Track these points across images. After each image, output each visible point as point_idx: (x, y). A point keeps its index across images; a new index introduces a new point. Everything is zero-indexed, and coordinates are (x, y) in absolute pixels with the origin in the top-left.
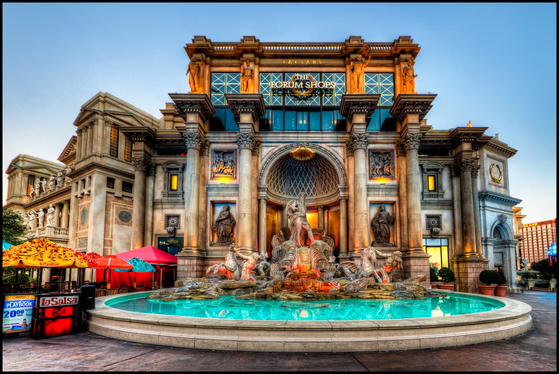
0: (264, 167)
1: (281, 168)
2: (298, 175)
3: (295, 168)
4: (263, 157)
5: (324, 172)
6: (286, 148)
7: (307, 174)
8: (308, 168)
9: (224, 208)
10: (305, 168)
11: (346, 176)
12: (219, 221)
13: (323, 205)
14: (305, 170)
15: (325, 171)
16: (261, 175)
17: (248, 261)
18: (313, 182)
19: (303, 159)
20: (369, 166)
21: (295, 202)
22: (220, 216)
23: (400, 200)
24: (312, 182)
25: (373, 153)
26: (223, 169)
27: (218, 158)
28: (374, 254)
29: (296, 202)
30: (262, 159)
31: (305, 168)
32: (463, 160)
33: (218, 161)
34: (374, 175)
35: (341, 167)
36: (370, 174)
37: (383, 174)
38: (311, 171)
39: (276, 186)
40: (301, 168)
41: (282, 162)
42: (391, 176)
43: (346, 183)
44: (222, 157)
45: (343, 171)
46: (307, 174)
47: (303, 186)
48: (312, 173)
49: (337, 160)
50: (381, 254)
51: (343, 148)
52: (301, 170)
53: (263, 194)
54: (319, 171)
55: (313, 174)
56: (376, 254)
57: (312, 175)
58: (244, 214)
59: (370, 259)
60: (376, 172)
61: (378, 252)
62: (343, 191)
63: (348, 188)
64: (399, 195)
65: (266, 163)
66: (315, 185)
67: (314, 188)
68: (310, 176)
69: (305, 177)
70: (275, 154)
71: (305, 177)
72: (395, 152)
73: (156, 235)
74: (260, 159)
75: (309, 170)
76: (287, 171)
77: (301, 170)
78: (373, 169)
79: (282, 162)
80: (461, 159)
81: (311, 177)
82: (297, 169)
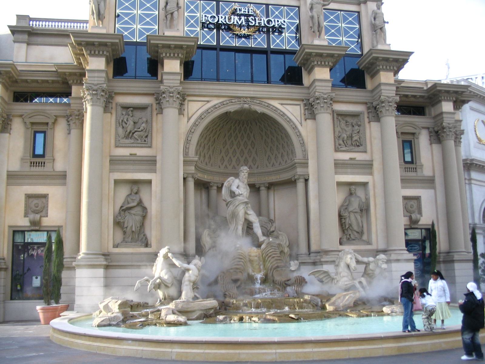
6: (222, 103)
25: (337, 115)
26: (133, 131)
27: (126, 116)
30: (189, 119)
32: (444, 124)
34: (340, 145)
36: (335, 145)
37: (352, 144)
44: (131, 115)
49: (292, 124)
51: (299, 107)
56: (356, 258)
65: (195, 124)
70: (207, 112)
72: (366, 115)
80: (442, 123)
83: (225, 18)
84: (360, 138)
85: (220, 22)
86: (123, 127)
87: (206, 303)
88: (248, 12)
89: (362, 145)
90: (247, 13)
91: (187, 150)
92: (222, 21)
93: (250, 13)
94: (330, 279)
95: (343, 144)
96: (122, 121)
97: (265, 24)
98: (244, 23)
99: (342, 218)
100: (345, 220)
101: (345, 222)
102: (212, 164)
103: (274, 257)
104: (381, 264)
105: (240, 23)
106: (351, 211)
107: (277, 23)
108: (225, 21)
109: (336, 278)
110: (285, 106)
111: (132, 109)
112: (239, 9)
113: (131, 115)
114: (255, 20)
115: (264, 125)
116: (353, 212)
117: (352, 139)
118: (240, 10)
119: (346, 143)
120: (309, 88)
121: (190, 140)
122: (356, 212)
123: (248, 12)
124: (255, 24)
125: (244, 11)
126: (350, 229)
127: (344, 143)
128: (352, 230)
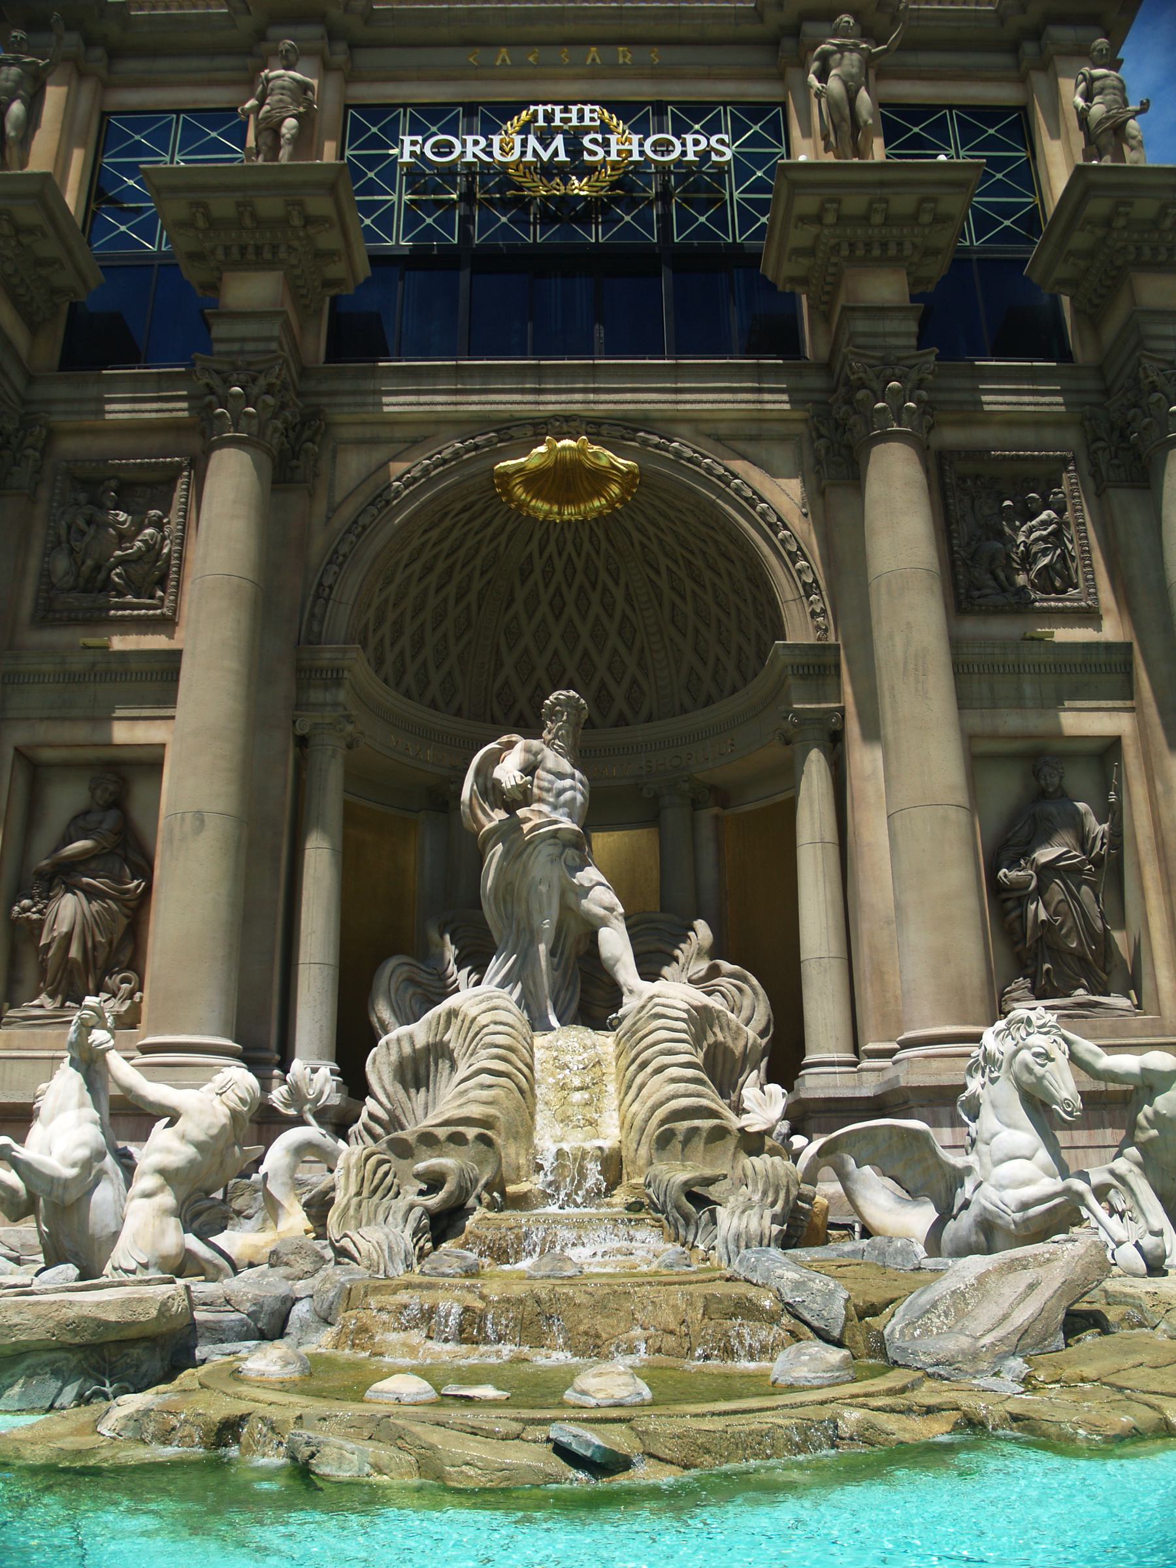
0: (344, 549)
1: (441, 566)
2: (544, 608)
4: (338, 498)
5: (689, 585)
7: (595, 597)
9: (92, 790)
10: (579, 565)
16: (323, 593)
19: (569, 512)
24: (622, 650)
28: (1062, 1059)
30: (333, 510)
38: (617, 583)
40: (559, 565)
41: (450, 530)
46: (595, 597)
48: (619, 594)
52: (558, 576)
55: (628, 599)
56: (1074, 1059)
61: (1086, 1047)
67: (634, 682)
68: (611, 616)
74: (321, 507)
75: (603, 576)
76: (477, 586)
77: (558, 576)
79: (450, 530)
81: (618, 616)
82: (537, 575)
83: (490, 145)
85: (469, 158)
86: (72, 551)
87: (98, 1304)
88: (581, 118)
90: (575, 122)
91: (316, 628)
92: (475, 155)
93: (587, 122)
95: (991, 583)
96: (69, 527)
97: (642, 153)
98: (562, 157)
99: (1008, 899)
102: (460, 709)
103: (659, 1070)
105: (545, 156)
107: (690, 149)
108: (490, 154)
109: (969, 1170)
110: (730, 443)
111: (113, 483)
112: (545, 111)
114: (606, 144)
115: (661, 541)
118: (549, 117)
120: (826, 367)
121: (331, 587)
123: (581, 118)
124: (608, 153)
125: (562, 120)
127: (996, 578)
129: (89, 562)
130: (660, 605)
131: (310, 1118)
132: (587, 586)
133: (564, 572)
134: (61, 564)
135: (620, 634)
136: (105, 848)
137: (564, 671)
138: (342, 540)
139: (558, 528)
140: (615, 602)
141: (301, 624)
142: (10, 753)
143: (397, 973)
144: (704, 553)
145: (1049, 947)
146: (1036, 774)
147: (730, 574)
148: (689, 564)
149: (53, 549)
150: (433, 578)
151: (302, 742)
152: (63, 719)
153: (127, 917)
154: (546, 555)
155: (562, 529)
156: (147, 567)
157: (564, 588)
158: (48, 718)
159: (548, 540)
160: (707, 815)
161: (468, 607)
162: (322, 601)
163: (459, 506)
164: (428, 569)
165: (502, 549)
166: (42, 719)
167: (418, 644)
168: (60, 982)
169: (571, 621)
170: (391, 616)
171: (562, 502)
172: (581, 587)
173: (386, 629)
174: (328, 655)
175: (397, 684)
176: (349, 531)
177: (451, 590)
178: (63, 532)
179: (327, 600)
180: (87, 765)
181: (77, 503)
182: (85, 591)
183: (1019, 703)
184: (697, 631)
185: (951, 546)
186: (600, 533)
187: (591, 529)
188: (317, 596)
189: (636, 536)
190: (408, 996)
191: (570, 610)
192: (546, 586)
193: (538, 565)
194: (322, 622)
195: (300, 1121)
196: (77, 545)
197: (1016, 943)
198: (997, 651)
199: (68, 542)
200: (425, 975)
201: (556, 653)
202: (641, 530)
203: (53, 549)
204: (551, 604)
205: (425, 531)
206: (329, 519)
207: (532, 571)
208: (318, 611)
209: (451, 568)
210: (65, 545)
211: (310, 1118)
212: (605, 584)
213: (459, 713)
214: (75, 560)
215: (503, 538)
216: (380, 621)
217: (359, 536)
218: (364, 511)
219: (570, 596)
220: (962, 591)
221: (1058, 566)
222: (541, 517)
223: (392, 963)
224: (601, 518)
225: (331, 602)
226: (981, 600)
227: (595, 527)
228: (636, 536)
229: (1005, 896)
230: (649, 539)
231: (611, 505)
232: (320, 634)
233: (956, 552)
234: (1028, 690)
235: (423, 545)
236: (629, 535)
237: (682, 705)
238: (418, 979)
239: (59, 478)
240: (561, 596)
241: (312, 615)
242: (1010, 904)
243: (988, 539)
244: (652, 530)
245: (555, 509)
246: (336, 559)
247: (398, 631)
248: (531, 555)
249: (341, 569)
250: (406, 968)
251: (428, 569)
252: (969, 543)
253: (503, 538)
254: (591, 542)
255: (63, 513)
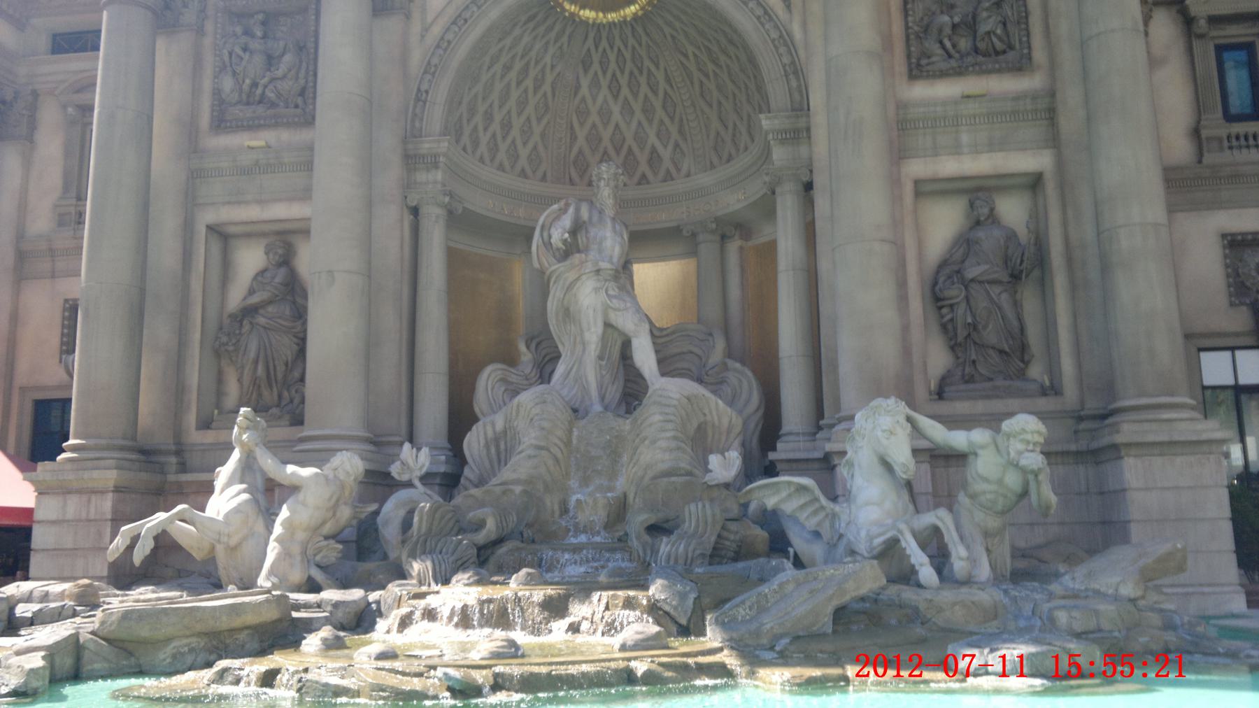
1: (518, 66)
3: (583, 62)
4: (429, 19)
7: (643, 80)
8: (643, 53)
10: (628, 55)
11: (796, 73)
12: (249, 312)
13: (717, 220)
14: (629, 65)
15: (715, 62)
16: (421, 97)
17: (301, 496)
18: (672, 119)
19: (612, 16)
20: (906, 14)
21: (571, 210)
22: (251, 292)
23: (1060, 165)
24: (667, 120)
27: (244, 39)
29: (578, 210)
30: (426, 29)
31: (628, 55)
33: (241, 53)
35: (774, 35)
38: (657, 66)
39: (503, 147)
42: (1011, 55)
43: (801, 107)
45: (782, 50)
47: (630, 141)
48: (660, 76)
50: (937, 432)
52: (613, 65)
53: (432, 180)
54: (693, 67)
57: (662, 85)
58: (330, 272)
59: (887, 465)
60: (941, 42)
62: (783, 142)
63: (808, 130)
64: (1054, 141)
65: (443, 45)
66: (681, 132)
68: (655, 92)
69: (635, 95)
71: (635, 95)
73: (23, 389)
74: (416, 28)
75: (647, 63)
76: (549, 78)
77: (613, 65)
78: (926, 29)
82: (596, 66)
84: (1004, 24)
89: (1011, 47)
91: (417, 124)
94: (821, 515)
95: (940, 51)
96: (230, 54)
100: (952, 310)
101: (952, 320)
104: (1020, 453)
106: (972, 280)
113: (259, 34)
116: (981, 282)
117: (975, 32)
119: (954, 46)
121: (427, 92)
122: (990, 282)
126: (975, 343)
128: (981, 346)
129: (248, 81)
130: (692, 83)
131: (417, 482)
132: (636, 72)
133: (617, 62)
134: (228, 84)
135: (664, 107)
136: (277, 296)
137: (624, 139)
138: (433, 54)
139: (607, 28)
140: (658, 82)
141: (406, 122)
142: (203, 230)
143: (493, 375)
144: (718, 41)
145: (975, 343)
146: (972, 205)
147: (737, 57)
148: (708, 49)
149: (220, 72)
150: (513, 75)
151: (415, 211)
152: (239, 203)
153: (298, 344)
154: (600, 49)
155: (610, 27)
156: (291, 83)
157: (618, 74)
158: (229, 203)
159: (601, 38)
160: (733, 247)
161: (545, 95)
162: (421, 103)
163: (524, 18)
164: (507, 68)
165: (565, 46)
166: (224, 204)
167: (507, 126)
168: (252, 393)
169: (626, 99)
170: (482, 108)
171: (605, 10)
172: (631, 73)
173: (478, 119)
174: (427, 146)
175: (492, 160)
176: (438, 46)
177: (529, 83)
178: (226, 58)
179: (425, 102)
180: (263, 235)
181: (235, 35)
182: (248, 103)
183: (956, 150)
184: (720, 103)
185: (907, 23)
186: (640, 30)
187: (631, 25)
188: (418, 99)
189: (667, 30)
190: (501, 393)
191: (625, 91)
192: (604, 73)
193: (596, 57)
194: (422, 120)
195: (409, 484)
196: (239, 69)
197: (951, 340)
198: (938, 109)
199: (231, 66)
200: (515, 376)
201: (617, 125)
202: (670, 24)
203: (220, 72)
204: (609, 87)
205: (500, 40)
206: (423, 37)
207: (591, 63)
208: (418, 111)
209: (528, 64)
210: (229, 69)
211: (417, 482)
212: (649, 70)
213: (544, 178)
214: (237, 79)
215: (565, 39)
216: (472, 111)
217: (445, 50)
218: (448, 29)
219: (623, 81)
220: (914, 60)
221: (999, 32)
222: (591, 21)
223: (488, 369)
224: (635, 17)
225: (428, 103)
226: (929, 68)
227: (635, 25)
228: (667, 30)
229: (940, 304)
230: (677, 31)
231: (642, 8)
232: (421, 128)
233: (911, 28)
234: (965, 138)
235: (501, 50)
236: (662, 30)
237: (711, 163)
238: (510, 379)
239: (219, 14)
240: (617, 81)
241: (415, 115)
242: (944, 311)
243: (942, 12)
244: (677, 24)
245: (601, 15)
246: (429, 69)
247: (489, 117)
248: (589, 50)
249: (434, 77)
250: (499, 372)
251: (507, 68)
252: (922, 19)
253: (565, 39)
254: (634, 36)
255: (225, 43)
